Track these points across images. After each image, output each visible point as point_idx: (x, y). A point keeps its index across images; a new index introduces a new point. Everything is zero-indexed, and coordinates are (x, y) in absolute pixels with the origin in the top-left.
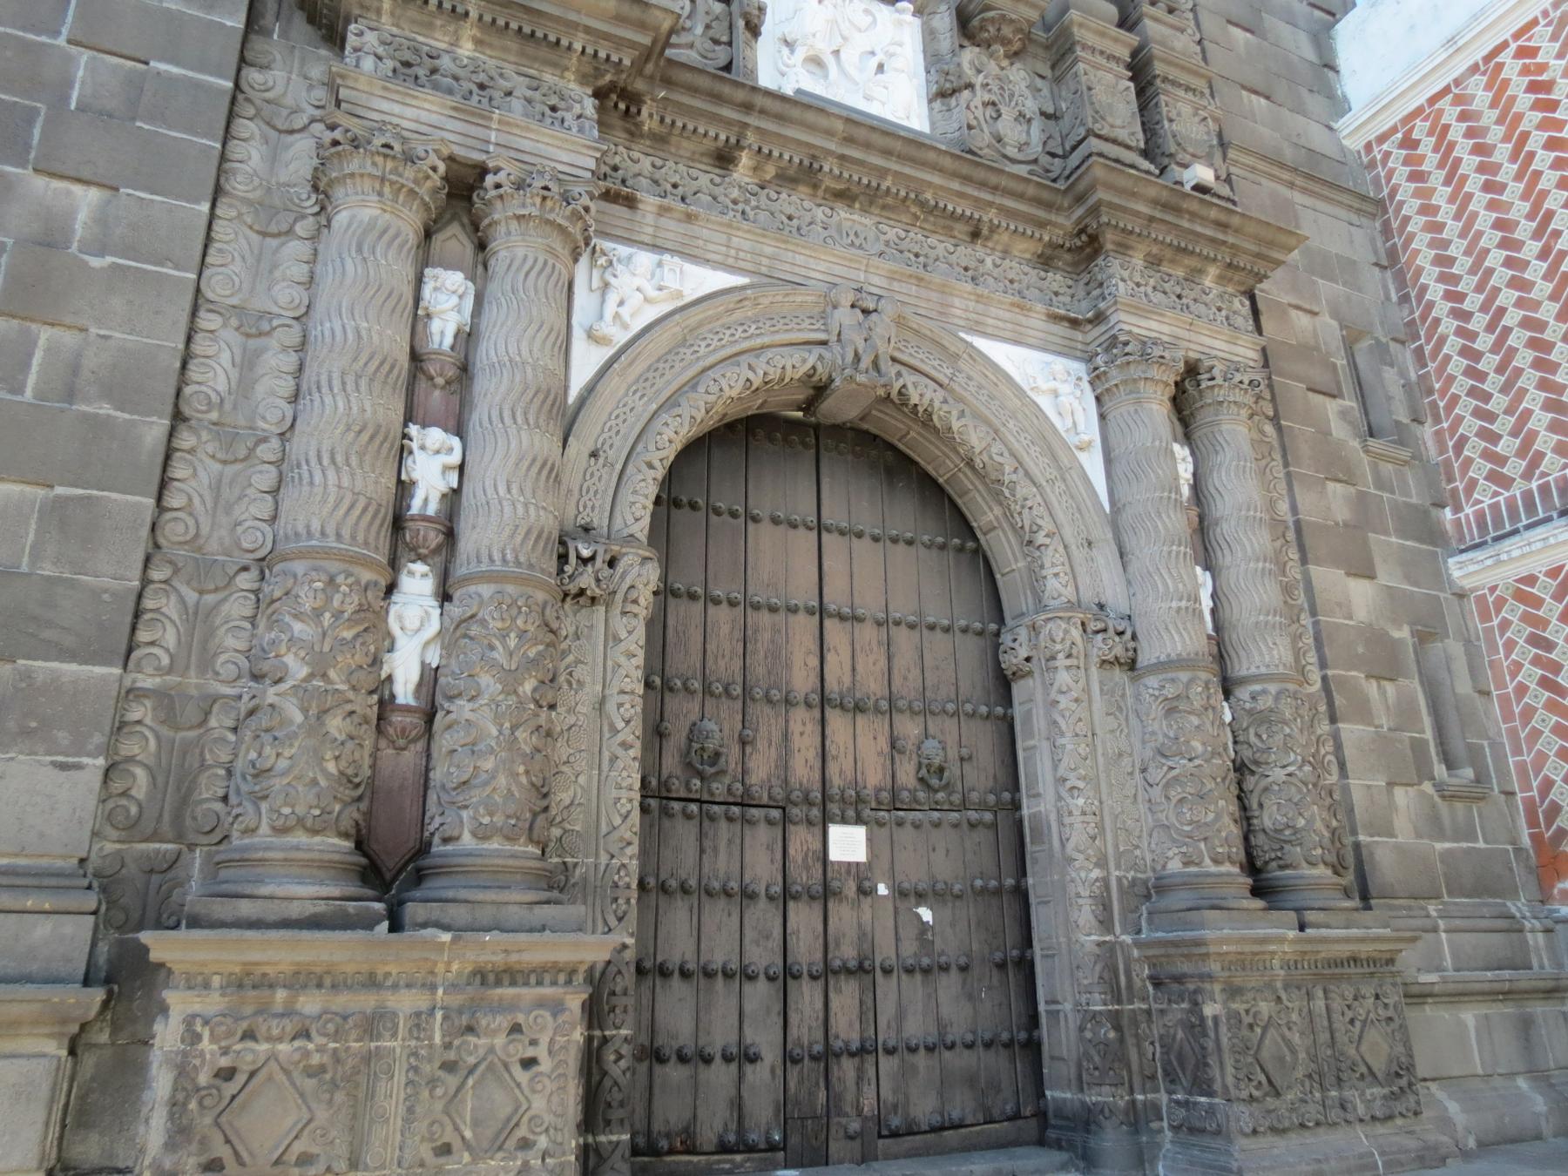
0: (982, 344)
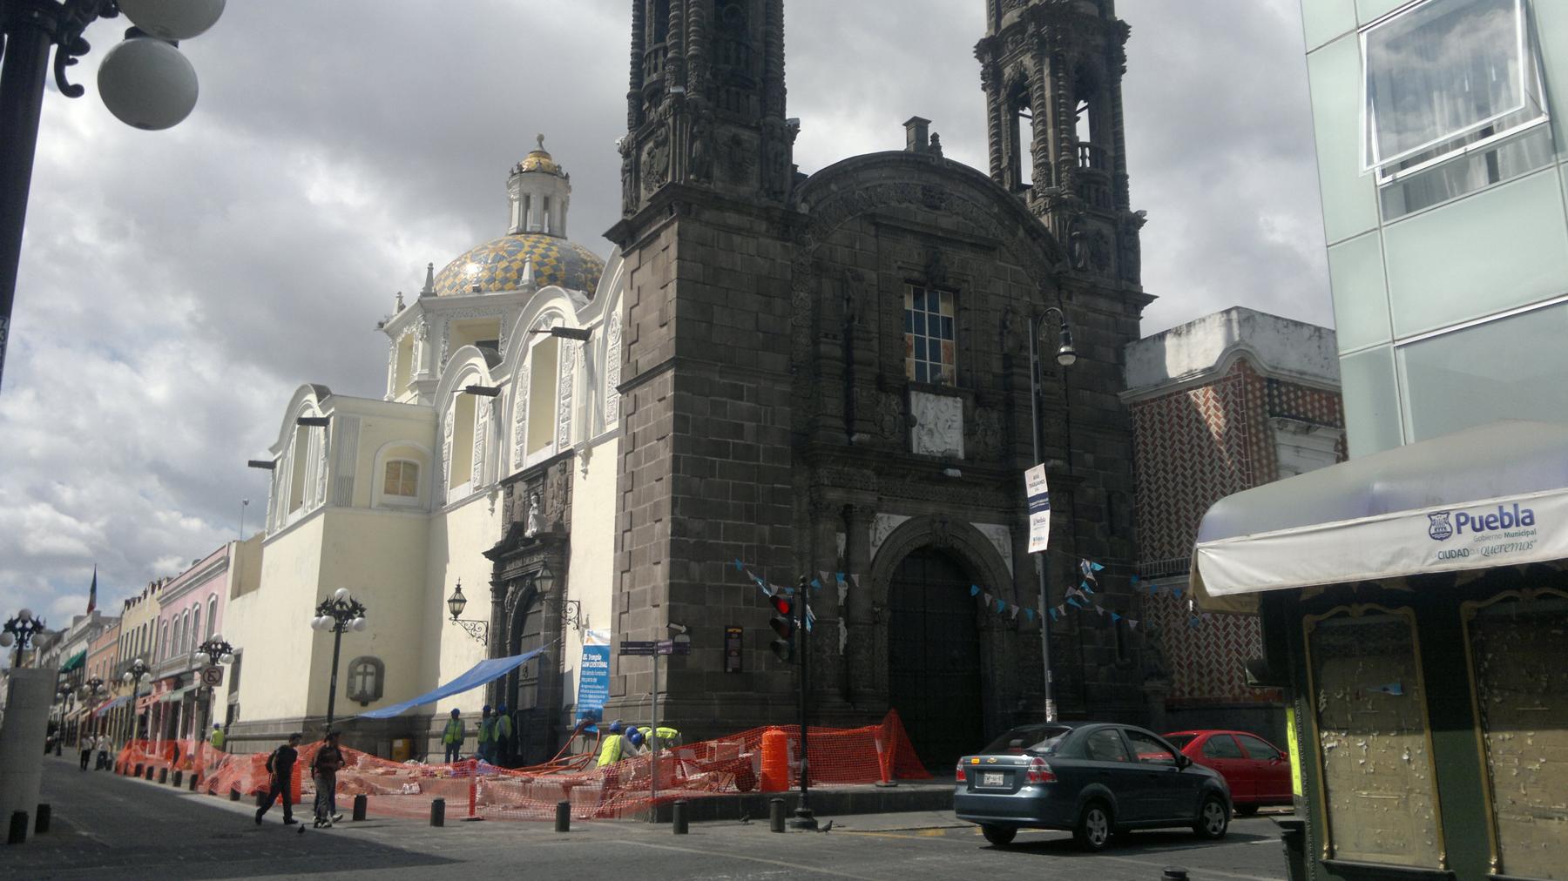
0: (977, 525)
